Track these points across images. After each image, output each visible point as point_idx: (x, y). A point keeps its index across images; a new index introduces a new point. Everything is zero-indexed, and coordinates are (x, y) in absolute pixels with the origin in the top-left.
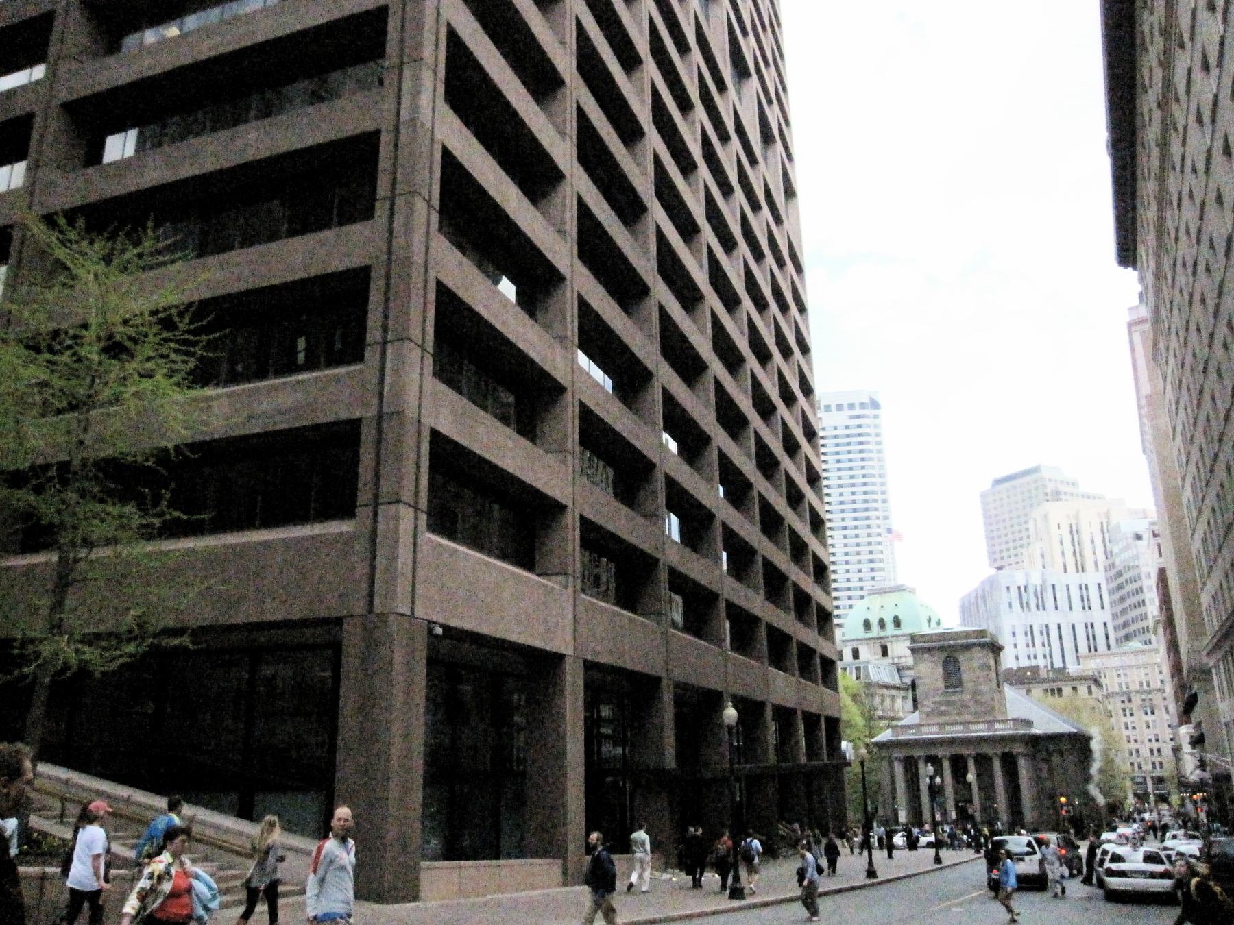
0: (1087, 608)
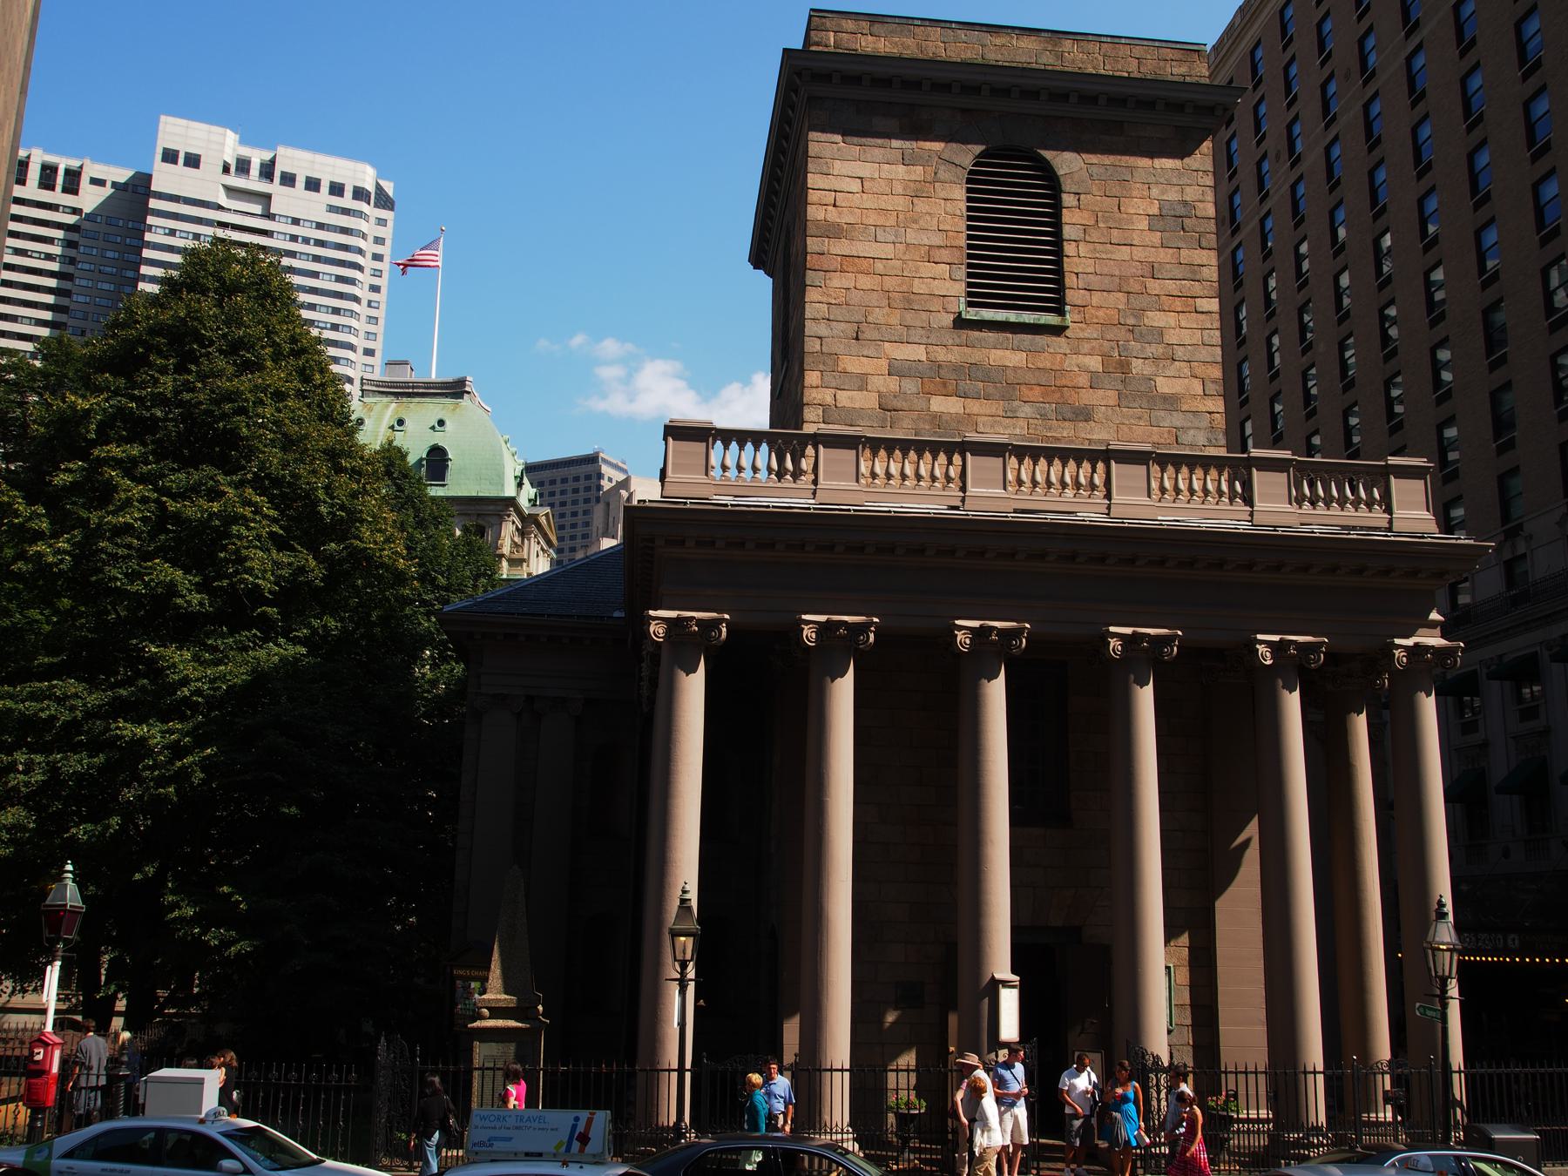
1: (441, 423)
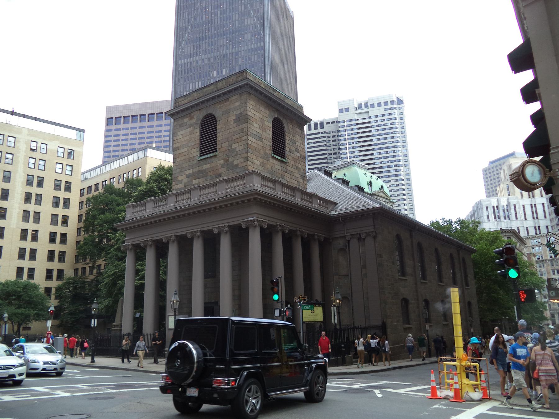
0: (536, 218)
1: (344, 174)
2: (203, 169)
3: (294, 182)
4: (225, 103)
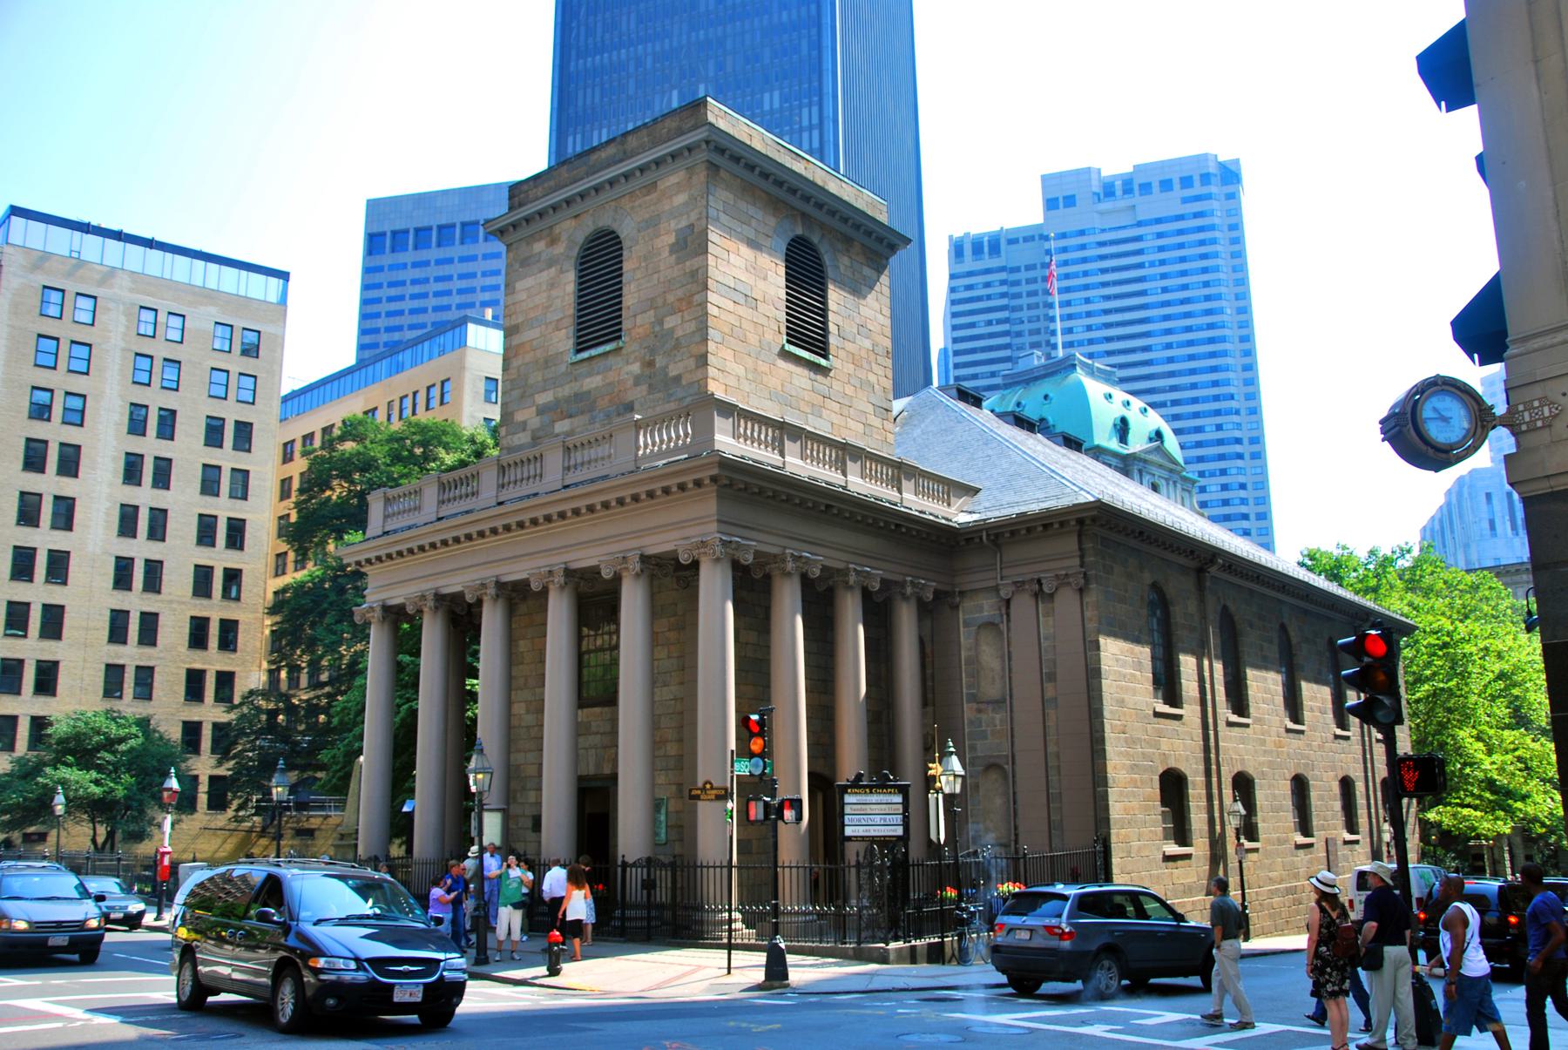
1: (1046, 397)
2: (585, 388)
3: (851, 424)
4: (648, 195)
